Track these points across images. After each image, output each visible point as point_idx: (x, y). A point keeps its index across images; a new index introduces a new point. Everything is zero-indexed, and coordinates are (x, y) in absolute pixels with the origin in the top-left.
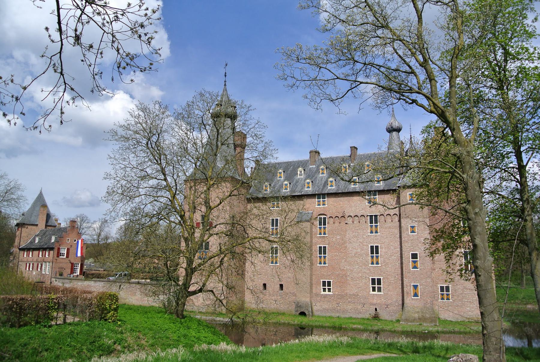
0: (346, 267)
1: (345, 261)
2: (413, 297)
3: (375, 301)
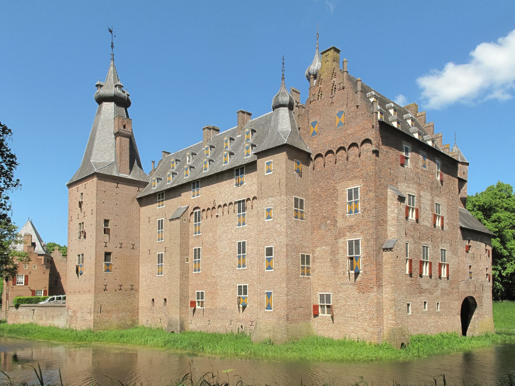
2: (266, 310)
3: (241, 316)
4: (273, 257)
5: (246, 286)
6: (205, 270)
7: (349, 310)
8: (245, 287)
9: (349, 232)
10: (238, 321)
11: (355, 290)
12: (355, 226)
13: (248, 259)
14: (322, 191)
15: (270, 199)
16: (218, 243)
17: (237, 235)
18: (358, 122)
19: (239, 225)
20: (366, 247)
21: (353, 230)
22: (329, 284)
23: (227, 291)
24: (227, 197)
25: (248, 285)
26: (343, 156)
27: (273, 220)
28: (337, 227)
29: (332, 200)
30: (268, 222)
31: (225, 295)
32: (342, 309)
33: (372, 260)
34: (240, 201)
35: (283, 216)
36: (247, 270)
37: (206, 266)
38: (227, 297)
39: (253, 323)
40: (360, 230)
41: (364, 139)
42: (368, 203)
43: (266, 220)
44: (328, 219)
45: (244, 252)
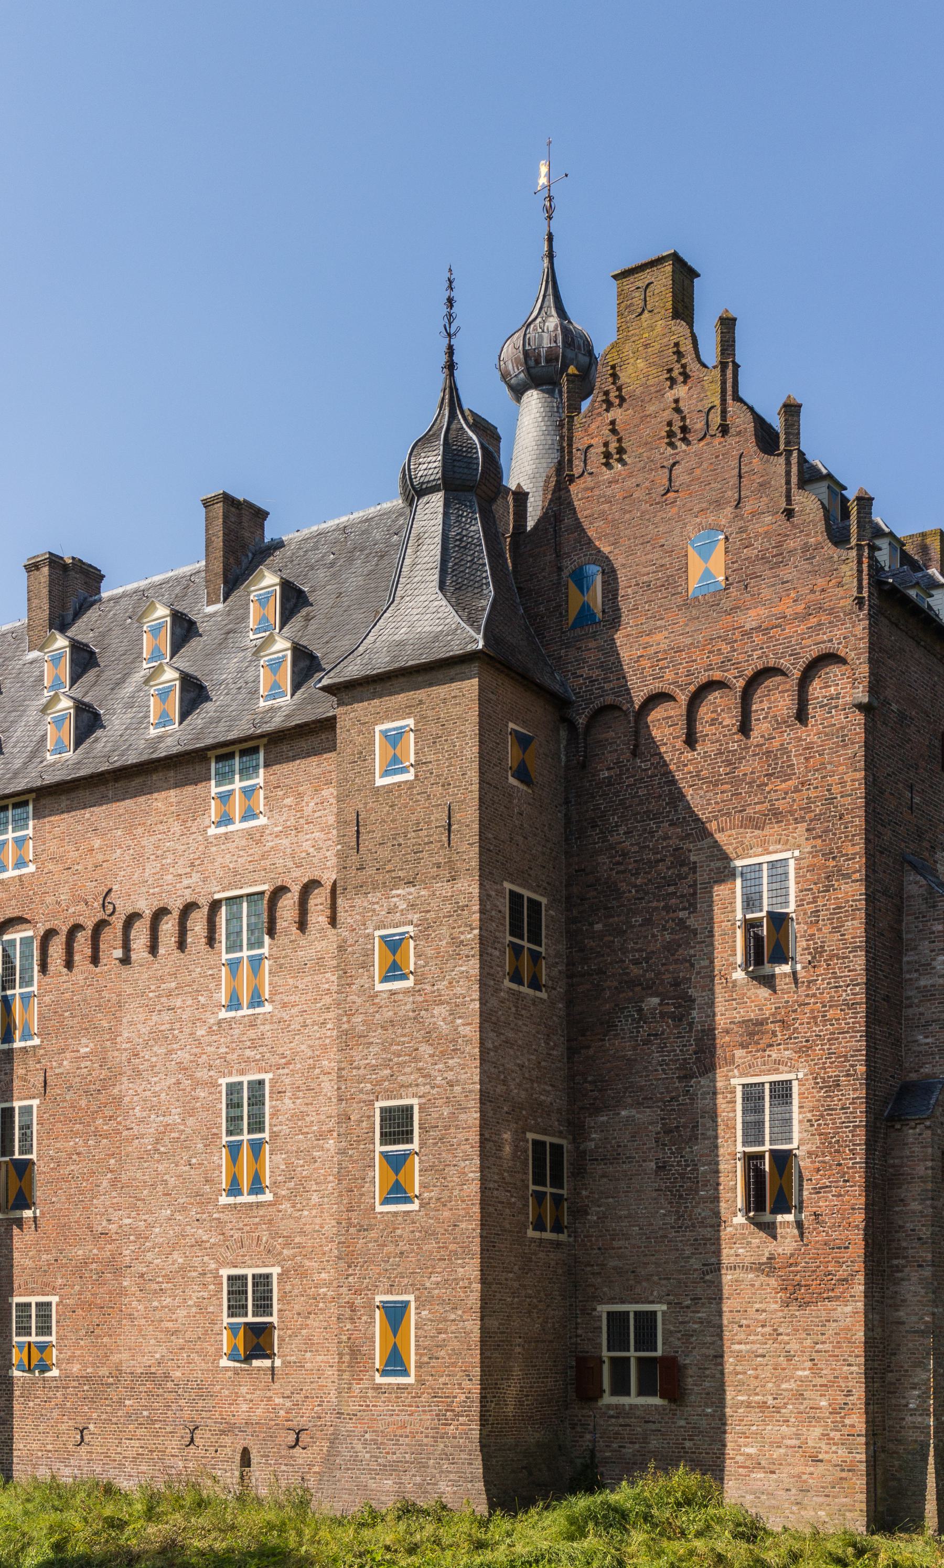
0: (115, 1216)
1: (114, 1183)
4: (415, 1146)
5: (268, 1276)
6: (58, 1206)
7: (740, 1376)
9: (743, 1048)
10: (228, 1429)
11: (769, 1291)
12: (772, 1022)
13: (279, 1158)
14: (622, 868)
15: (398, 892)
16: (125, 1086)
17: (223, 1050)
18: (787, 582)
19: (234, 1003)
20: (822, 1113)
21: (765, 1041)
22: (651, 1268)
23: (168, 1300)
24: (170, 877)
26: (720, 723)
27: (418, 987)
28: (691, 1024)
29: (667, 908)
30: (393, 993)
31: (158, 1315)
32: (707, 1372)
33: (848, 1168)
34: (241, 897)
35: (463, 969)
36: (270, 1204)
37: (65, 1186)
38: (170, 1325)
39: (303, 1436)
40: (795, 1038)
41: (815, 654)
42: (833, 928)
43: (379, 987)
44: (650, 989)
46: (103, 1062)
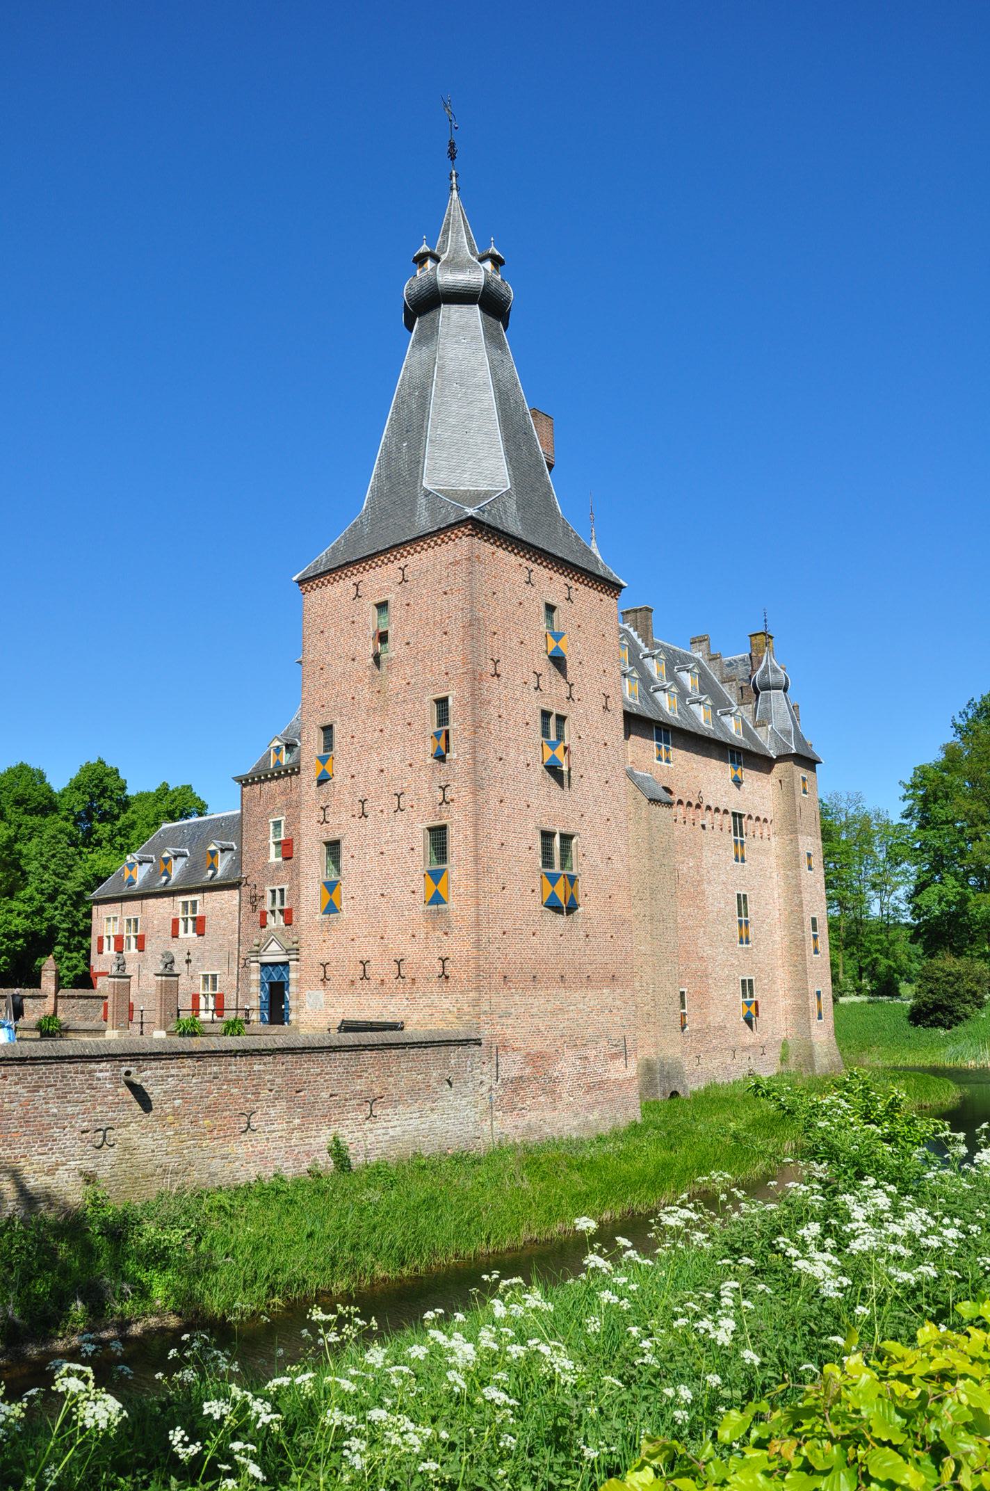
1: (705, 933)
8: (750, 981)
25: (753, 978)
45: (746, 916)
46: (698, 872)
